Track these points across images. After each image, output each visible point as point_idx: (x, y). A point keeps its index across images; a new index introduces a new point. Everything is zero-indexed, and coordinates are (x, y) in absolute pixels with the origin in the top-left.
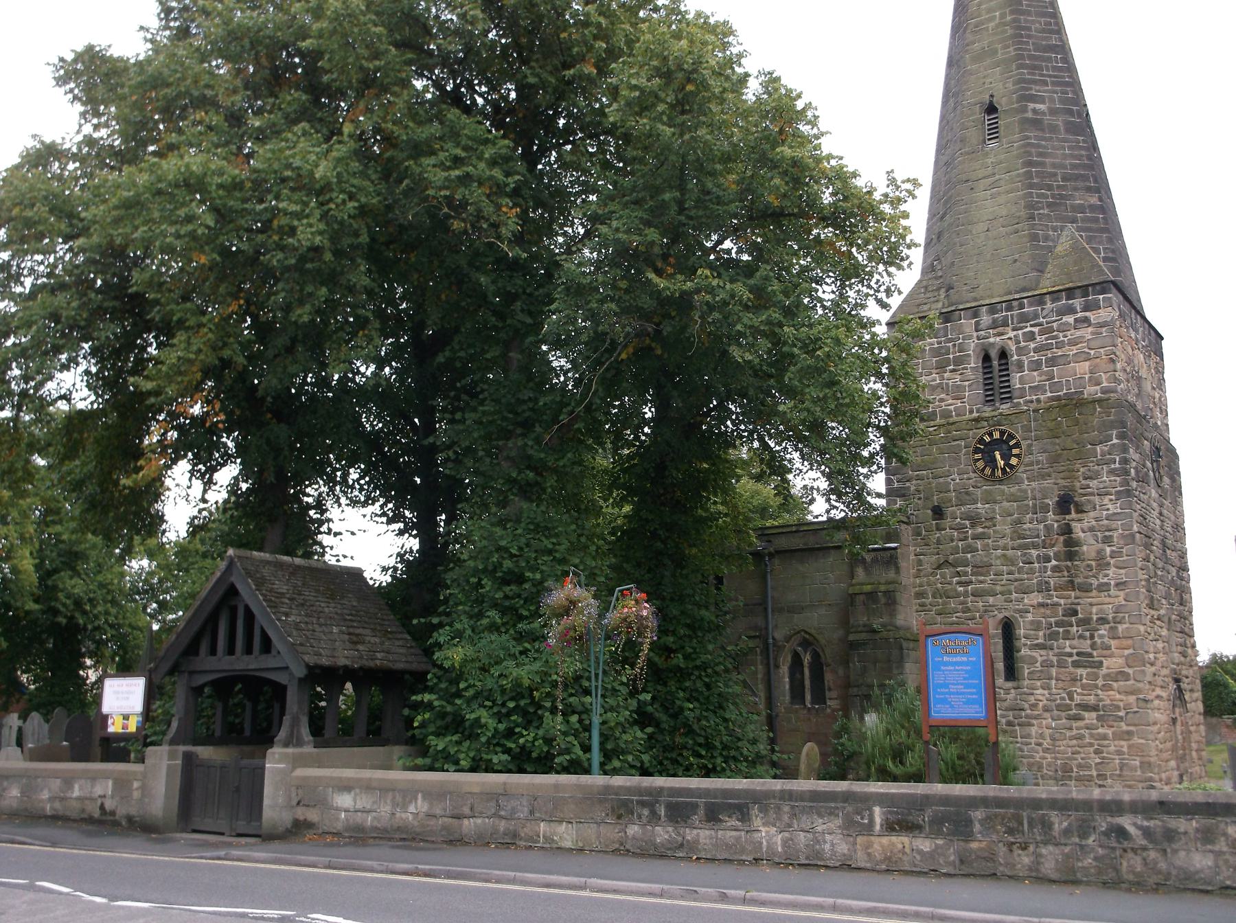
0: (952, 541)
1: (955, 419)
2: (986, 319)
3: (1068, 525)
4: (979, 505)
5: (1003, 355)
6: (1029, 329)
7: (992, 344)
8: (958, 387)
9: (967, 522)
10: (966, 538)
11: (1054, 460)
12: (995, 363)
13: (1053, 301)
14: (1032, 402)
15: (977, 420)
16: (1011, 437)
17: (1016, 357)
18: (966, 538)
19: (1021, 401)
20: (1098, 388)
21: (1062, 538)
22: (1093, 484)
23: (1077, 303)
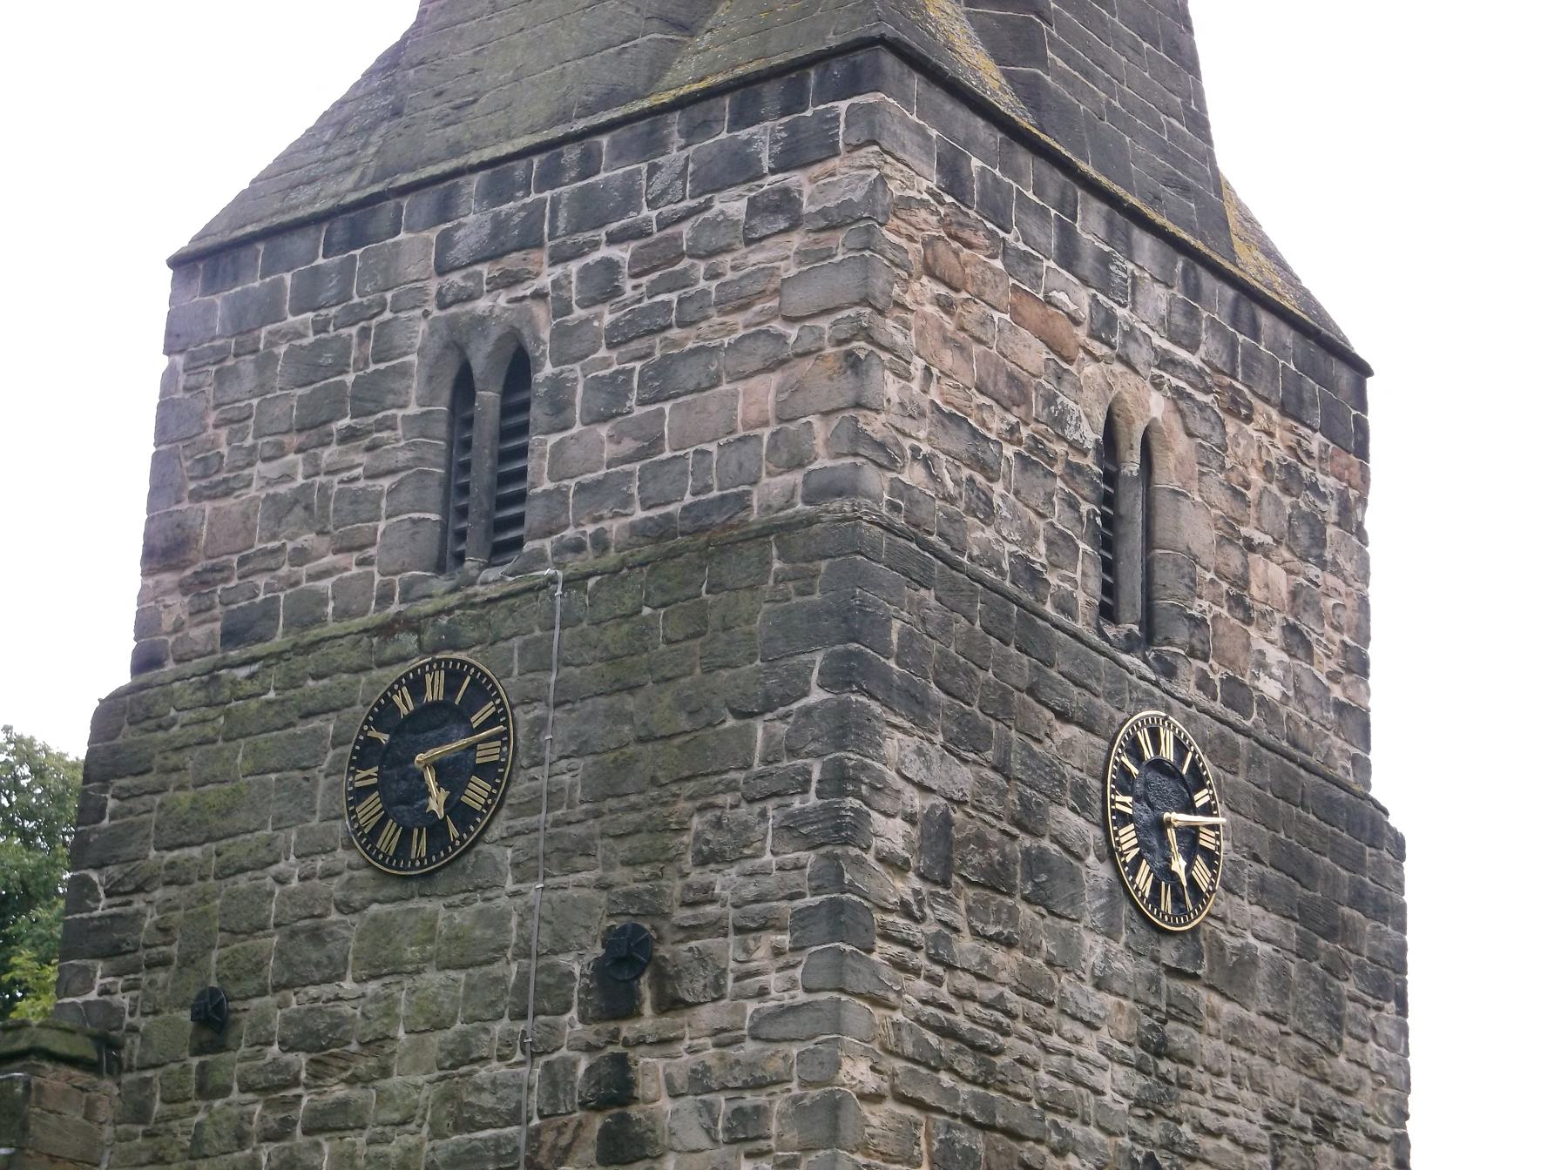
0: (241, 1140)
1: (332, 628)
2: (473, 223)
3: (621, 1062)
4: (348, 985)
5: (518, 368)
6: (604, 252)
7: (481, 321)
8: (357, 498)
9: (301, 1059)
10: (281, 1133)
11: (607, 787)
12: (488, 397)
13: (692, 134)
14: (578, 547)
15: (386, 630)
16: (482, 690)
17: (548, 369)
18: (281, 1133)
19: (547, 544)
20: (797, 477)
21: (598, 1121)
22: (725, 880)
23: (763, 137)
